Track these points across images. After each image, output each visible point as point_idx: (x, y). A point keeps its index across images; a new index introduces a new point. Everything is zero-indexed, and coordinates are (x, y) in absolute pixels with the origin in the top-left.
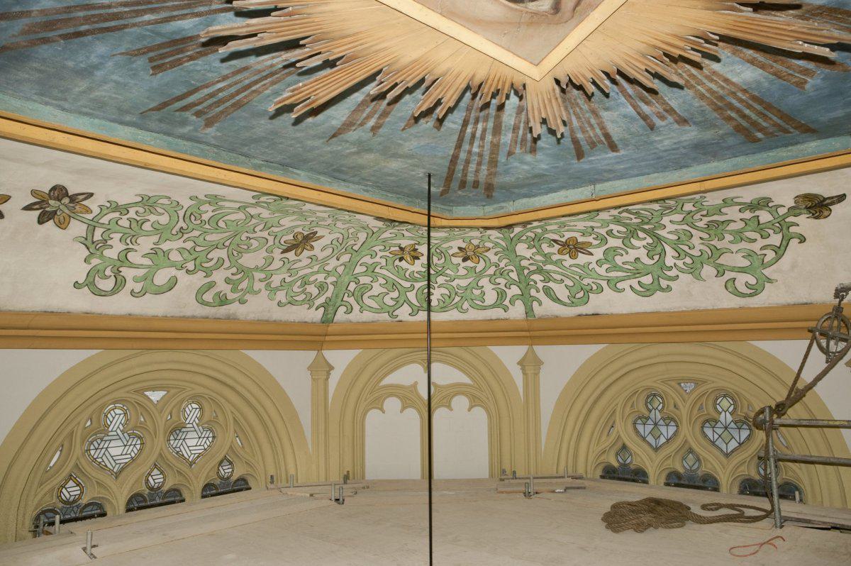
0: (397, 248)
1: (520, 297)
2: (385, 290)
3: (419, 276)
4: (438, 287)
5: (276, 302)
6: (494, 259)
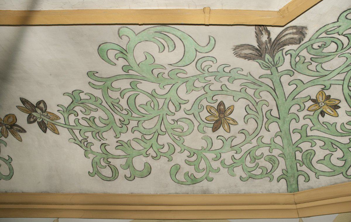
0: (310, 103)
2: (327, 152)
5: (238, 177)
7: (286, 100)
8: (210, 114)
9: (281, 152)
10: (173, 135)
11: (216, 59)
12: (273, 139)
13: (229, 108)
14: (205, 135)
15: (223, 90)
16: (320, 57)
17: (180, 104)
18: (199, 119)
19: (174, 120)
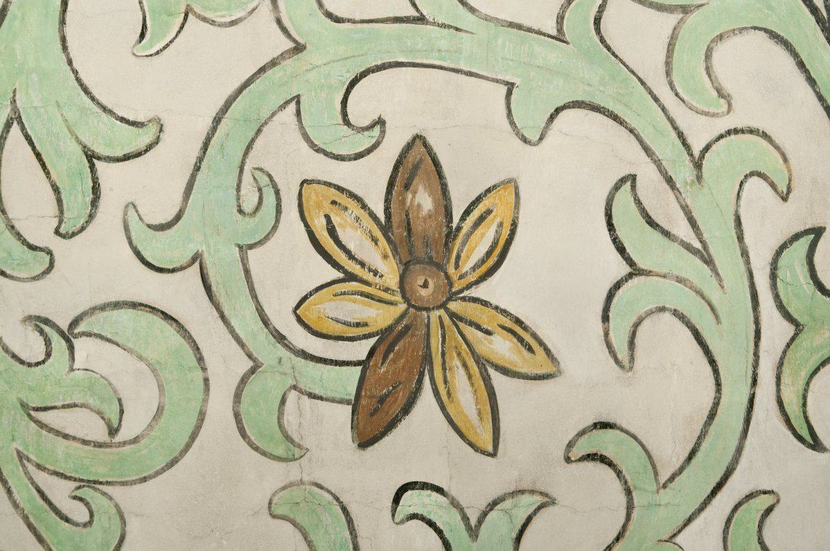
10: (30, 468)
13: (476, 214)
14: (293, 472)
15: (421, 19)
17: (91, 157)
19: (47, 321)
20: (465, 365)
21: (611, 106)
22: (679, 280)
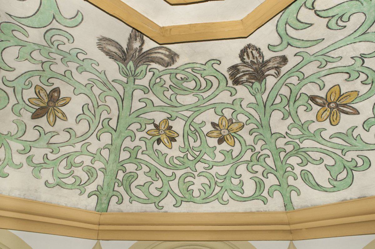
0: (152, 127)
1: (278, 188)
2: (149, 179)
3: (179, 163)
4: (199, 176)
5: (42, 181)
6: (249, 139)
7: (130, 115)
8: (38, 96)
9: (103, 166)
11: (74, 39)
12: (100, 151)
14: (19, 118)
15: (65, 76)
16: (178, 88)
18: (19, 97)
20: (53, 115)
21: (89, 96)
22: (90, 117)
